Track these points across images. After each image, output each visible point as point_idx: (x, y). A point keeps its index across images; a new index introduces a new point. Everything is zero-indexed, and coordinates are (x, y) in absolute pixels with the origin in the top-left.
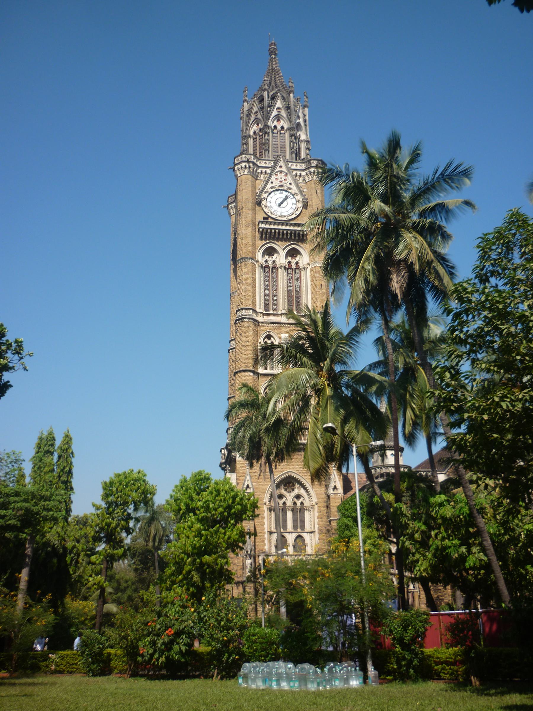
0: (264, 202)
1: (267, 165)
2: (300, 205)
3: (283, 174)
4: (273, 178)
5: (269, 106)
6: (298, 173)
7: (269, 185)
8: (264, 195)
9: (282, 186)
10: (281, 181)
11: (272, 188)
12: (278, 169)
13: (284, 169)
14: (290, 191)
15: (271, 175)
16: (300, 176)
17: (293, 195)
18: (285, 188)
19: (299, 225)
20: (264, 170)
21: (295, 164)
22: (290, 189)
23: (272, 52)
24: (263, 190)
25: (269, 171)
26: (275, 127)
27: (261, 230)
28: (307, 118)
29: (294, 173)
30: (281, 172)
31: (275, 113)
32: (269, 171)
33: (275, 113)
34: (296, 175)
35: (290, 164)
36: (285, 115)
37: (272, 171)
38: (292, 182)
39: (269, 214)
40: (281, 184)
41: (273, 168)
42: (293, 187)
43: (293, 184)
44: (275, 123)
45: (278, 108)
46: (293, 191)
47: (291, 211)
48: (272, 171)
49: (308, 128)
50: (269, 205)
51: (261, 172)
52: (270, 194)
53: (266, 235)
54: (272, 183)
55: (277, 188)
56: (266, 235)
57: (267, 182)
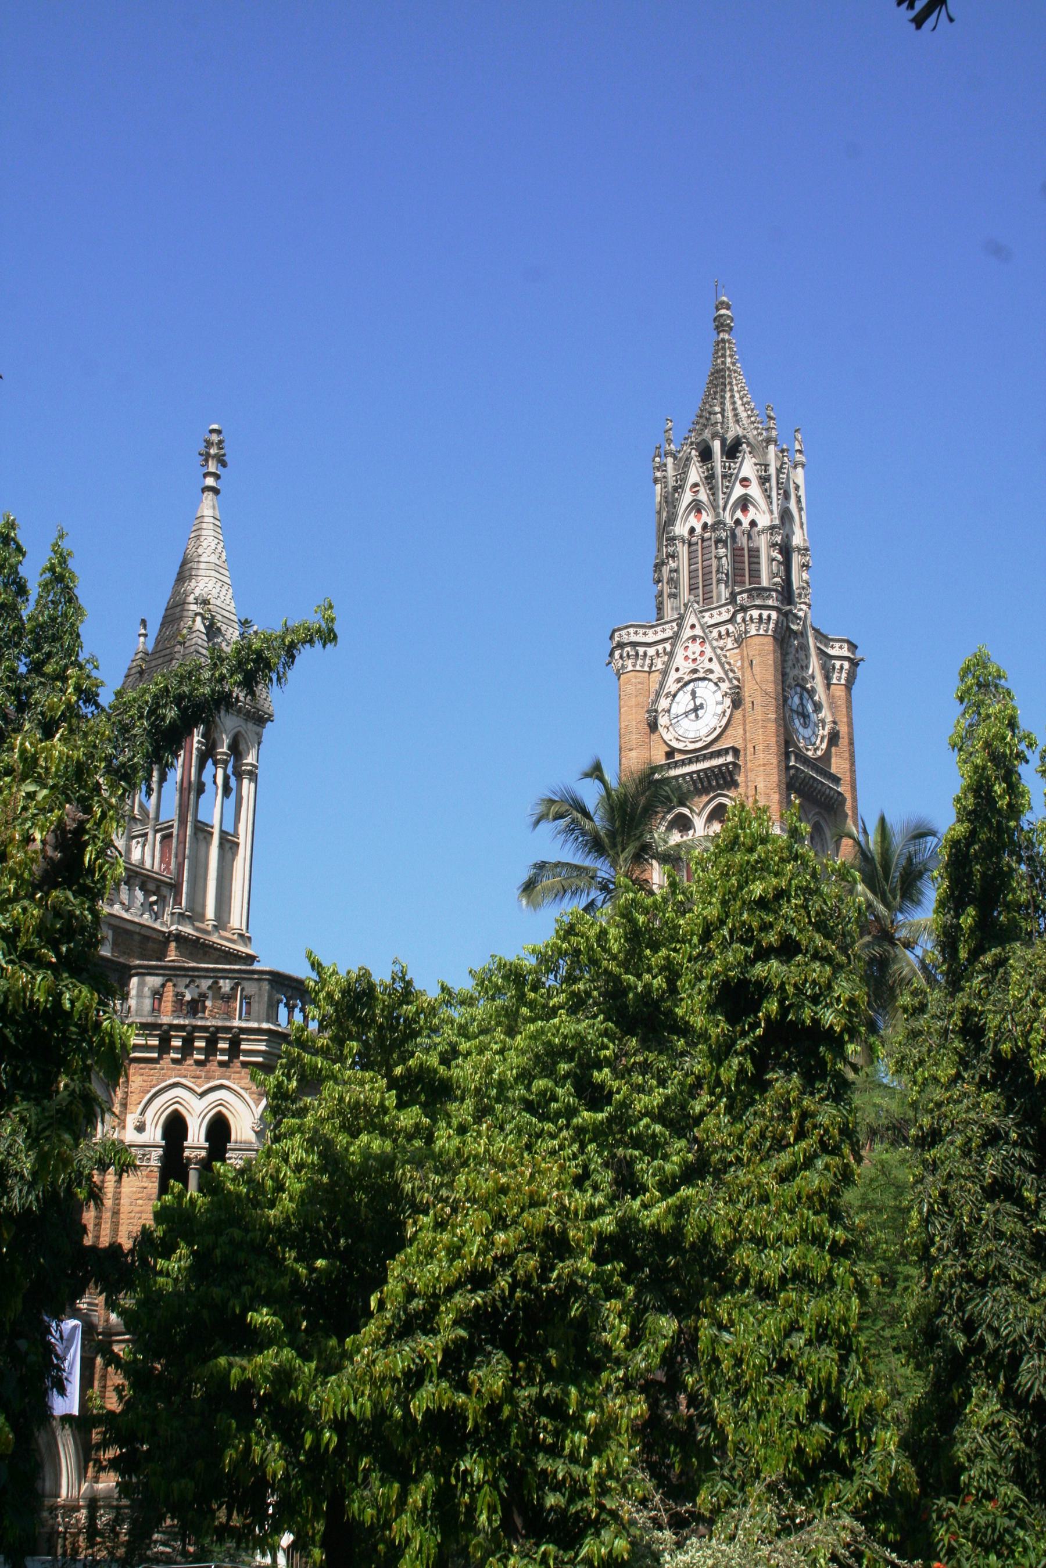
0: (663, 721)
1: (661, 636)
2: (728, 702)
3: (698, 641)
4: (679, 660)
5: (675, 489)
6: (723, 629)
7: (673, 676)
8: (664, 703)
9: (695, 671)
10: (694, 660)
11: (678, 680)
12: (688, 633)
13: (698, 631)
14: (710, 676)
15: (671, 655)
16: (728, 634)
17: (716, 684)
18: (701, 675)
20: (660, 648)
21: (715, 612)
22: (711, 671)
23: (721, 325)
24: (658, 695)
25: (668, 648)
26: (692, 530)
30: (694, 638)
33: (687, 497)
35: (707, 614)
37: (673, 645)
40: (693, 666)
41: (676, 636)
42: (715, 666)
44: (693, 521)
45: (696, 485)
48: (673, 645)
51: (658, 653)
52: (674, 696)
54: (677, 670)
55: (687, 678)
57: (665, 673)
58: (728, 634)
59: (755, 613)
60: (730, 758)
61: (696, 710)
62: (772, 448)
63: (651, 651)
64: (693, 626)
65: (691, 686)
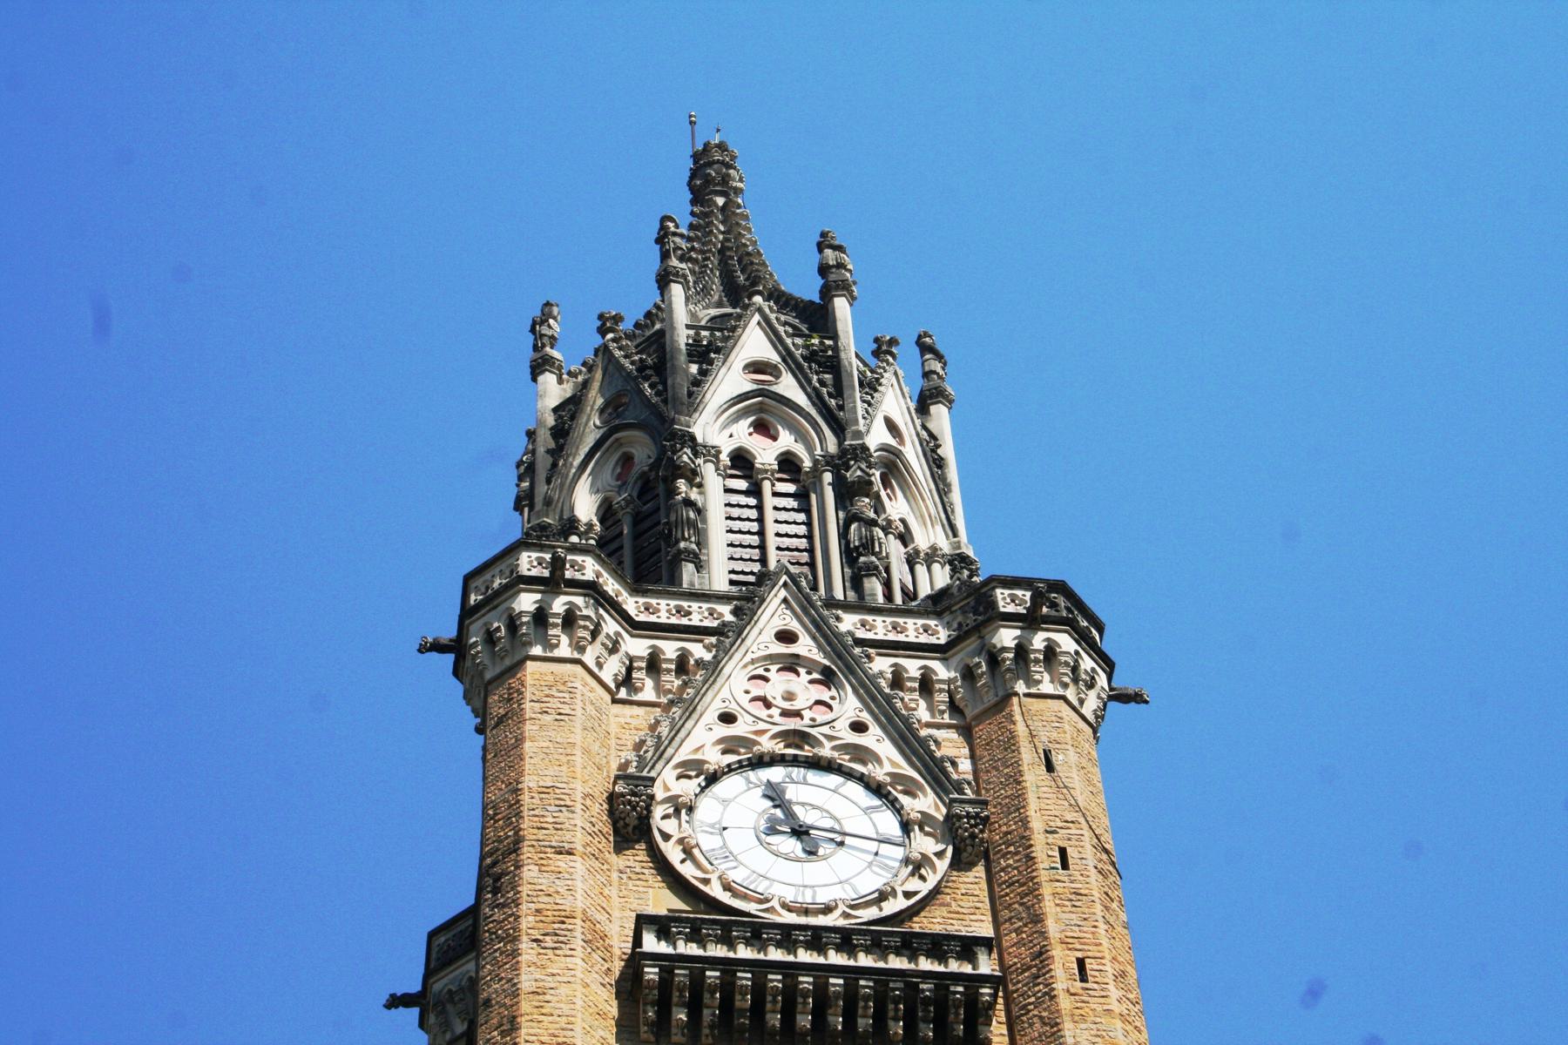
6: (913, 667)
9: (798, 738)
11: (730, 745)
16: (926, 685)
17: (877, 789)
18: (826, 751)
19: (937, 946)
20: (670, 649)
27: (651, 973)
28: (948, 450)
29: (881, 665)
30: (791, 664)
31: (730, 380)
32: (698, 651)
34: (898, 681)
36: (801, 399)
37: (722, 653)
38: (865, 717)
39: (716, 891)
40: (792, 724)
43: (875, 730)
45: (756, 367)
46: (879, 773)
47: (870, 883)
49: (956, 496)
50: (707, 842)
51: (654, 664)
52: (713, 779)
53: (695, 1008)
55: (767, 745)
56: (695, 1008)
58: (926, 685)
59: (1066, 642)
60: (986, 965)
61: (800, 832)
62: (939, 412)
63: (638, 647)
64: (786, 637)
65: (776, 774)
